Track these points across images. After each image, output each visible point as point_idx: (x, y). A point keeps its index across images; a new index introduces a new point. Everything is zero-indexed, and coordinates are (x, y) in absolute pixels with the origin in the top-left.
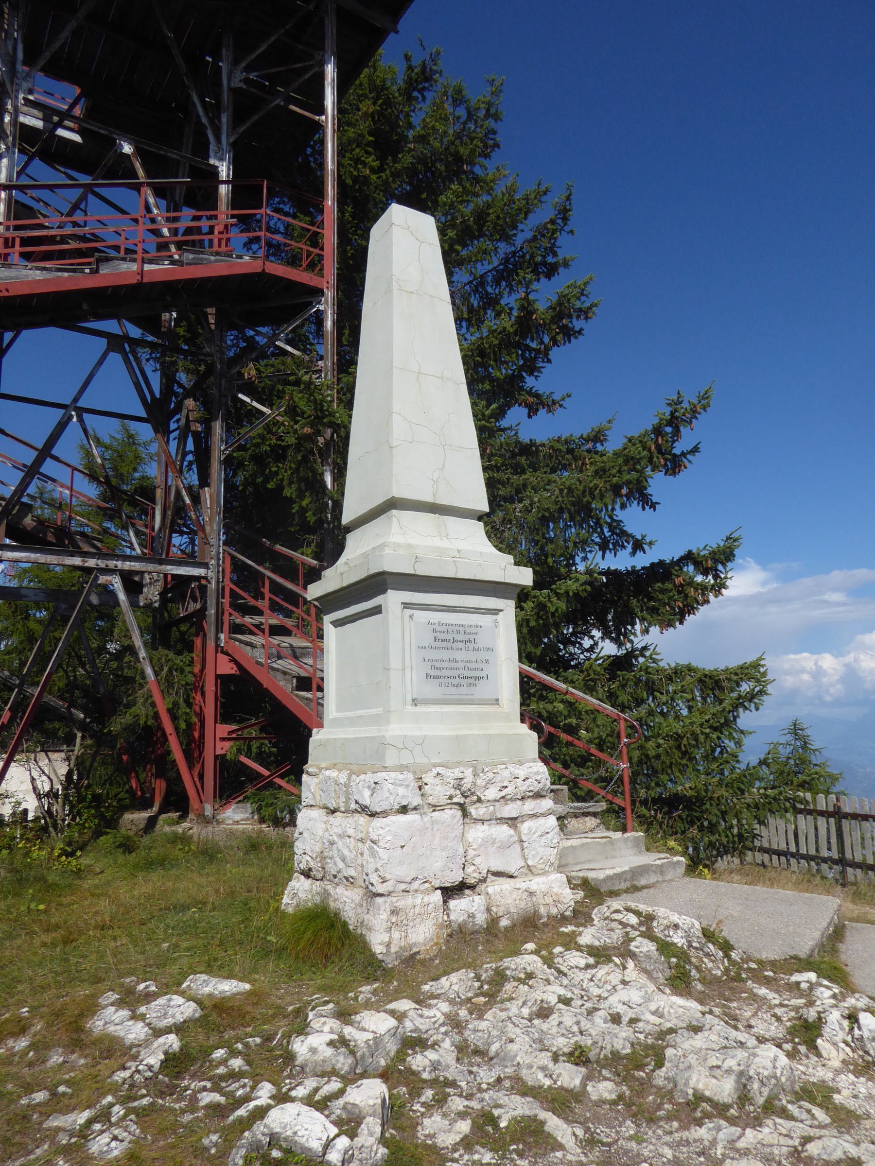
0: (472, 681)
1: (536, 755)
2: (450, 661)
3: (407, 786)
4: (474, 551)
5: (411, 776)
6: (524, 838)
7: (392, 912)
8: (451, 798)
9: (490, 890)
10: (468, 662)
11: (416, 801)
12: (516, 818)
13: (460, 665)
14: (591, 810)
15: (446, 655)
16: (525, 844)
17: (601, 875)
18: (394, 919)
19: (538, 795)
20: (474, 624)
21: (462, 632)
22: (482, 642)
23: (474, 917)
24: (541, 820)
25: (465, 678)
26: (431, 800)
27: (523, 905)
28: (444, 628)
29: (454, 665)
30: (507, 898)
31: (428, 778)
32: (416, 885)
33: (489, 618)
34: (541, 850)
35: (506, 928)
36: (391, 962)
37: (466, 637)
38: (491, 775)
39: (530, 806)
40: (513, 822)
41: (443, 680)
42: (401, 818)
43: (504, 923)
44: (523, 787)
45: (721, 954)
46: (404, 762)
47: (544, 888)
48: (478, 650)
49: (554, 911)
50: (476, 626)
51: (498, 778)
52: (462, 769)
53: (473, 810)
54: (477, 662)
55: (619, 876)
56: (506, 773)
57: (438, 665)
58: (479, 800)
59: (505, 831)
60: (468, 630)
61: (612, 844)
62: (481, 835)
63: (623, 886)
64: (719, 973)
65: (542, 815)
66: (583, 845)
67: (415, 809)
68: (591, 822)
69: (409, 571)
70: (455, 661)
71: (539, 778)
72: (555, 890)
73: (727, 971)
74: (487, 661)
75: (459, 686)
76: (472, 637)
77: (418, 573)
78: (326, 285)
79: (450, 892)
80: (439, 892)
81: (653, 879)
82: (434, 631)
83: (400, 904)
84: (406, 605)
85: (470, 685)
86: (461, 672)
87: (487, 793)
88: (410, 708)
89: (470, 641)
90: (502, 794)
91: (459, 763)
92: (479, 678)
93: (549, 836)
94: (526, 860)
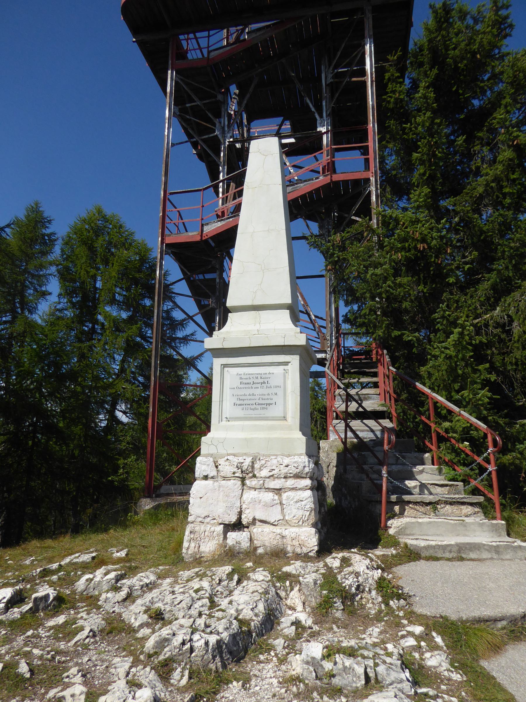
0: (265, 406)
1: (304, 451)
2: (250, 395)
3: (208, 465)
4: (281, 329)
5: (212, 459)
6: (284, 502)
7: (191, 532)
8: (234, 473)
9: (255, 530)
10: (263, 395)
11: (213, 473)
12: (280, 489)
14: (465, 500)
15: (248, 392)
16: (285, 506)
17: (423, 544)
18: (192, 536)
19: (297, 476)
20: (268, 372)
22: (272, 383)
23: (240, 543)
24: (300, 492)
26: (222, 474)
27: (275, 542)
28: (248, 376)
30: (265, 537)
31: (221, 461)
32: (208, 520)
33: (282, 368)
34: (295, 511)
35: (260, 554)
36: (187, 558)
37: (262, 381)
38: (263, 462)
39: (290, 483)
40: (278, 491)
41: (244, 406)
42: (204, 482)
43: (260, 551)
44: (285, 470)
45: (380, 599)
46: (211, 452)
47: (293, 535)
48: (270, 387)
49: (298, 550)
50: (270, 373)
51: (269, 464)
52: (244, 457)
53: (248, 482)
54: (268, 394)
55: (444, 548)
56: (275, 461)
57: (241, 398)
58: (254, 476)
59: (270, 496)
60: (263, 376)
61: (465, 526)
62: (251, 496)
63: (447, 555)
64: (373, 612)
65: (300, 489)
66: (430, 523)
67: (212, 478)
68: (468, 509)
69: (220, 346)
70: (253, 395)
71: (296, 465)
72: (303, 538)
73: (380, 611)
74: (276, 394)
75: (255, 409)
76: (266, 381)
77: (226, 346)
78: (371, 174)
79: (229, 527)
80: (222, 526)
81: (485, 555)
82: (241, 378)
83: (197, 529)
84: (225, 366)
85: (263, 408)
87: (261, 472)
88: (224, 423)
89: (264, 383)
90: (271, 474)
91: (245, 454)
92: (269, 404)
93: (303, 503)
94: (284, 516)
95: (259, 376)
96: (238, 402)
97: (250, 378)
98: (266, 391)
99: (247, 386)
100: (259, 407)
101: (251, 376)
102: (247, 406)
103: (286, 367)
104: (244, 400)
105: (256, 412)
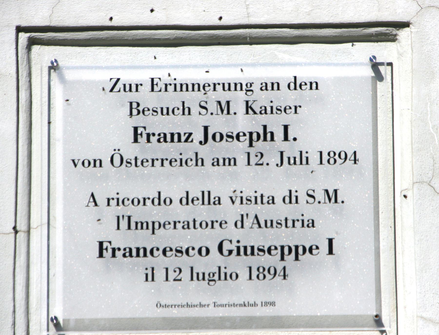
0: (272, 260)
2: (187, 200)
10: (259, 199)
13: (230, 212)
15: (175, 183)
20: (284, 75)
21: (239, 107)
25: (250, 251)
28: (172, 99)
29: (203, 213)
41: (159, 262)
48: (302, 159)
50: (296, 84)
57: (139, 213)
60: (261, 99)
70: (207, 199)
74: (333, 196)
75: (222, 275)
76: (275, 124)
82: (135, 109)
85: (264, 273)
86: (232, 233)
89: (266, 135)
92: (297, 252)
95: (238, 99)
96: (123, 239)
97: (186, 110)
98: (275, 181)
99: (171, 150)
100: (238, 264)
101: (193, 99)
102: (172, 261)
103: (383, 51)
104: (154, 227)
105: (225, 292)
